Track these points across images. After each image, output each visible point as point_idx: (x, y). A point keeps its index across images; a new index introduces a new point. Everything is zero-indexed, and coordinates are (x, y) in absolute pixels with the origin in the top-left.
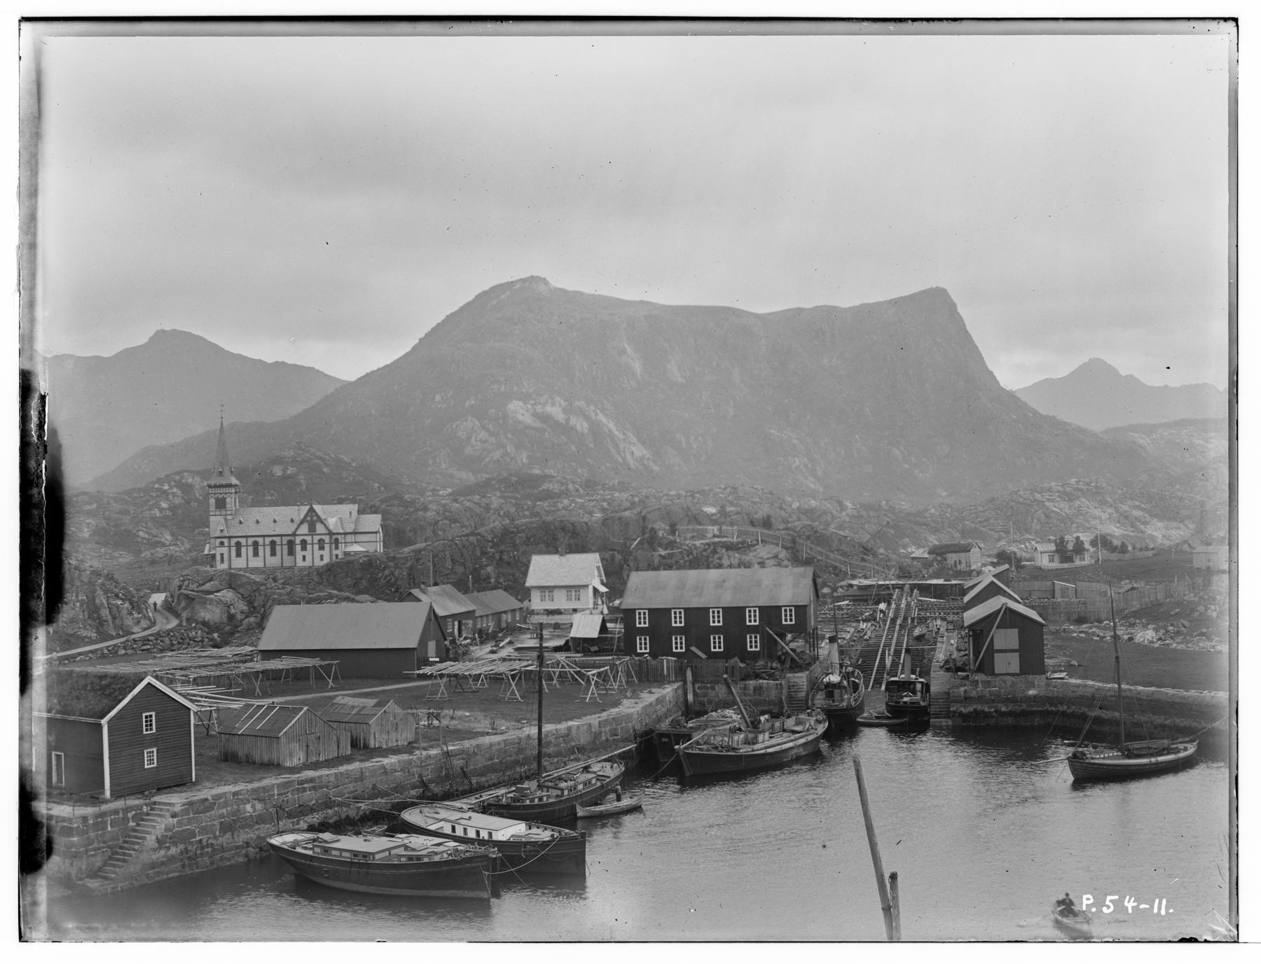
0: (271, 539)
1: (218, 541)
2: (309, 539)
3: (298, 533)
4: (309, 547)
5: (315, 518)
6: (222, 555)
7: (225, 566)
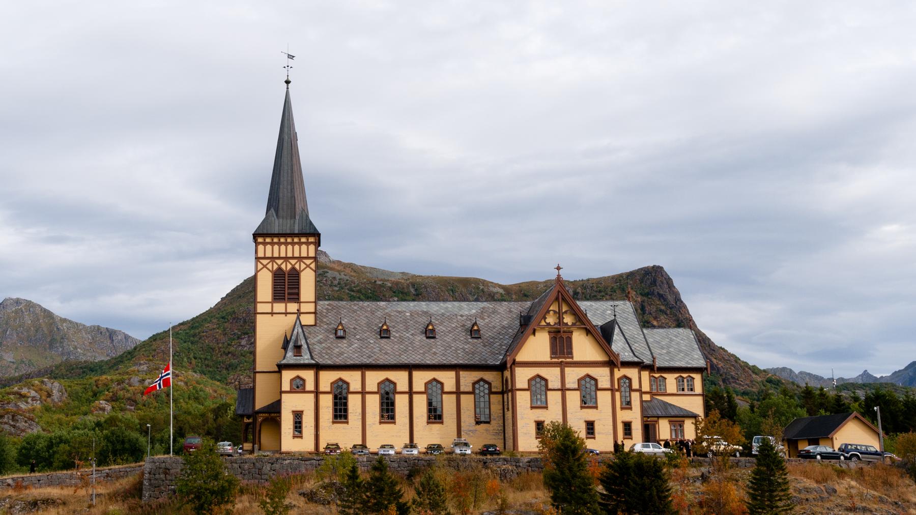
0: (429, 375)
1: (288, 376)
2: (552, 375)
3: (521, 357)
4: (554, 398)
5: (568, 320)
6: (298, 416)
7: (305, 445)
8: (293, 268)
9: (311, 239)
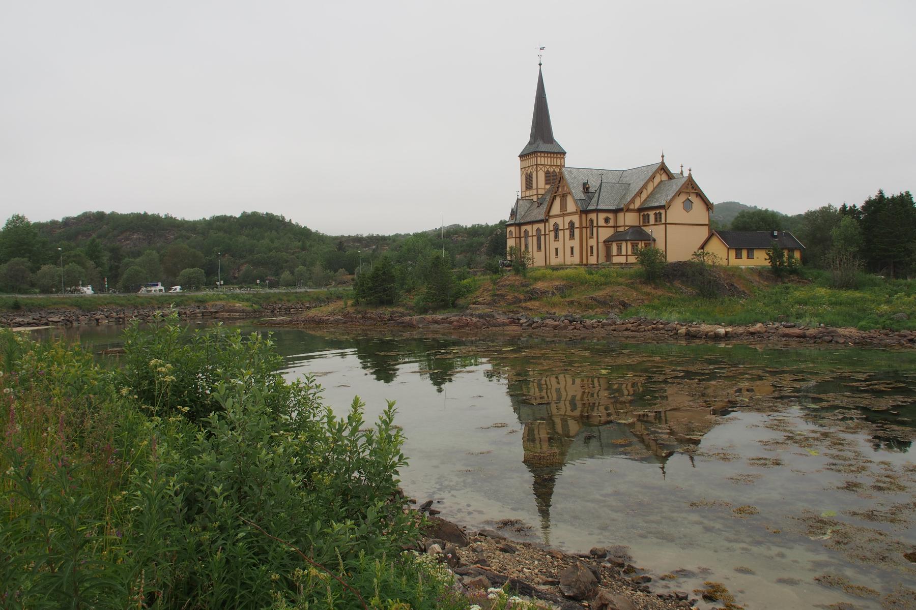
8: (554, 171)
9: (562, 156)
